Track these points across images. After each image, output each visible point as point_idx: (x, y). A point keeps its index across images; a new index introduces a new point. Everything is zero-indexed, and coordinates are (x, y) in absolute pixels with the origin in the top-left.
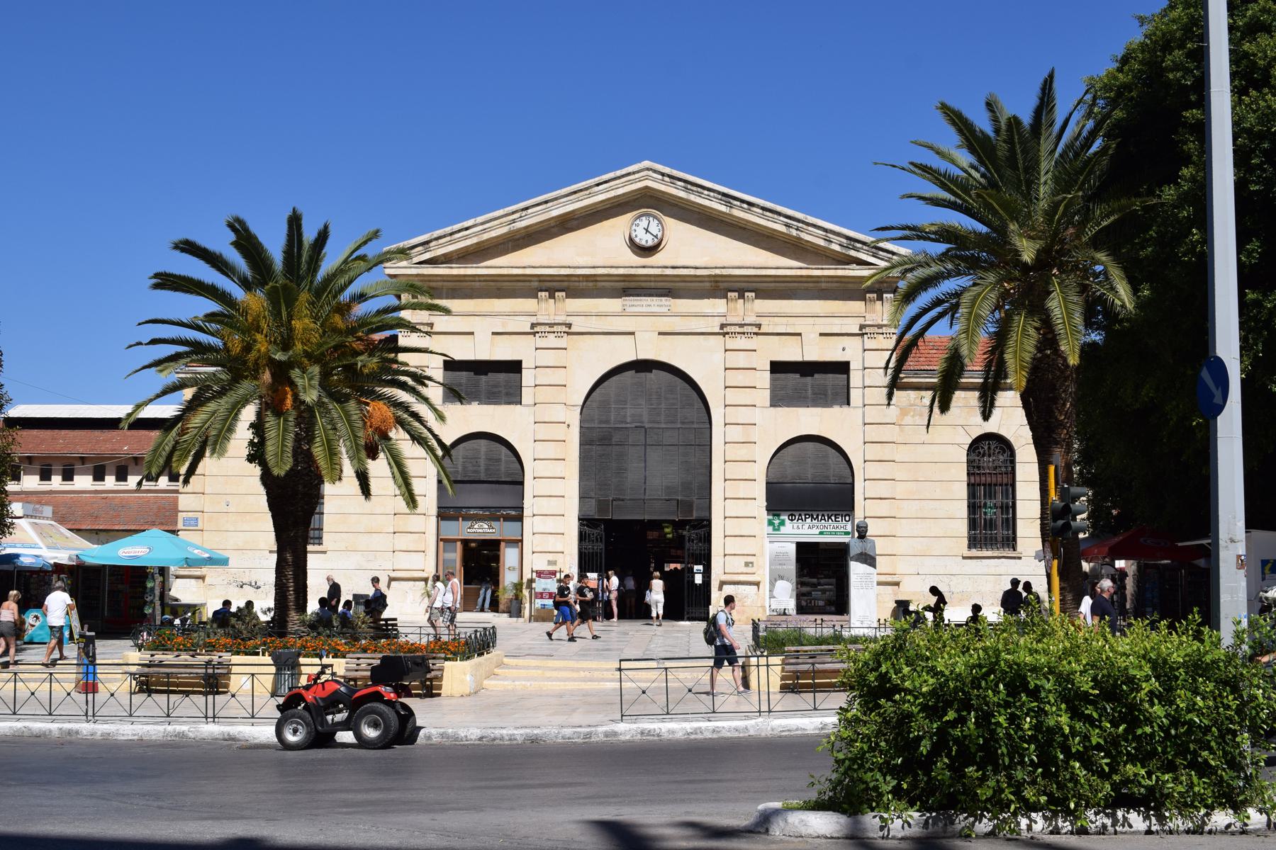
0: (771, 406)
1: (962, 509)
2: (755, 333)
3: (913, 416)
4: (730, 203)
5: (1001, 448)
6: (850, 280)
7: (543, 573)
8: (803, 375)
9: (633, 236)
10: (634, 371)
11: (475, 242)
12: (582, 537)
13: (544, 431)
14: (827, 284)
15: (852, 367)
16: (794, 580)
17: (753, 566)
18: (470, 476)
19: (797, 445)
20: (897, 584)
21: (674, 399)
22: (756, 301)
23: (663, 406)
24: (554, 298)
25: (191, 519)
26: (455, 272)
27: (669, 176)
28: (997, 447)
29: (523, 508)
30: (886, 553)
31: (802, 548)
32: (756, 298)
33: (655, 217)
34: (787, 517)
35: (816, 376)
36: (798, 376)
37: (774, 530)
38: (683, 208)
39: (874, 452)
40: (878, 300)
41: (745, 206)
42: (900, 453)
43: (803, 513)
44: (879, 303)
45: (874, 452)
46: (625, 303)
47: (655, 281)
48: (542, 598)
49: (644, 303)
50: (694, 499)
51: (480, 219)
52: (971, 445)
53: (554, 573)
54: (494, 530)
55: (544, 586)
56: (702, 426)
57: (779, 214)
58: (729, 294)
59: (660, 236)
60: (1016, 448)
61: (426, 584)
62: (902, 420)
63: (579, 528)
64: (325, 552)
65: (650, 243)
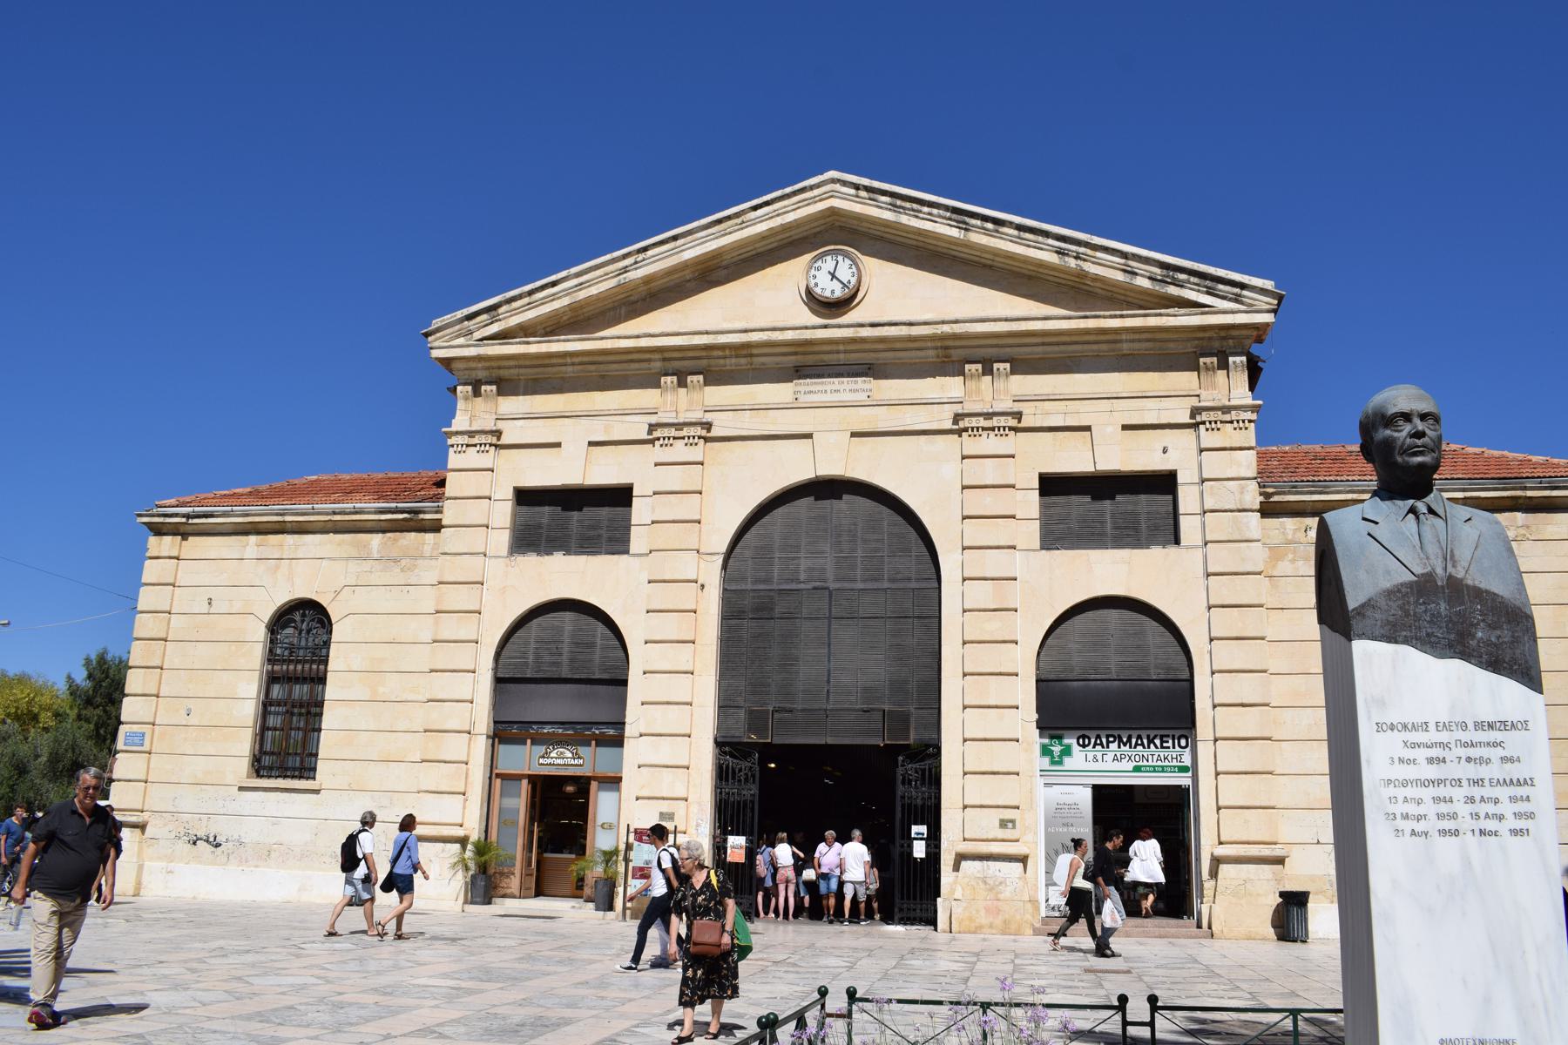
0: (1042, 548)
2: (1011, 429)
3: (1293, 561)
6: (1170, 336)
8: (1097, 497)
10: (812, 498)
12: (723, 774)
14: (1132, 345)
15: (1180, 479)
17: (1014, 827)
19: (1090, 614)
20: (1280, 861)
21: (878, 541)
22: (1011, 377)
23: (859, 553)
25: (135, 734)
26: (533, 349)
27: (868, 189)
30: (1258, 804)
31: (1103, 795)
32: (1013, 372)
33: (846, 255)
34: (1075, 741)
35: (1119, 498)
36: (1087, 499)
38: (891, 242)
39: (1225, 622)
40: (1219, 368)
41: (990, 226)
43: (1103, 734)
44: (1221, 374)
45: (1225, 622)
49: (828, 388)
50: (912, 709)
51: (574, 270)
56: (924, 585)
57: (1046, 234)
61: (464, 848)
62: (1274, 567)
65: (839, 293)
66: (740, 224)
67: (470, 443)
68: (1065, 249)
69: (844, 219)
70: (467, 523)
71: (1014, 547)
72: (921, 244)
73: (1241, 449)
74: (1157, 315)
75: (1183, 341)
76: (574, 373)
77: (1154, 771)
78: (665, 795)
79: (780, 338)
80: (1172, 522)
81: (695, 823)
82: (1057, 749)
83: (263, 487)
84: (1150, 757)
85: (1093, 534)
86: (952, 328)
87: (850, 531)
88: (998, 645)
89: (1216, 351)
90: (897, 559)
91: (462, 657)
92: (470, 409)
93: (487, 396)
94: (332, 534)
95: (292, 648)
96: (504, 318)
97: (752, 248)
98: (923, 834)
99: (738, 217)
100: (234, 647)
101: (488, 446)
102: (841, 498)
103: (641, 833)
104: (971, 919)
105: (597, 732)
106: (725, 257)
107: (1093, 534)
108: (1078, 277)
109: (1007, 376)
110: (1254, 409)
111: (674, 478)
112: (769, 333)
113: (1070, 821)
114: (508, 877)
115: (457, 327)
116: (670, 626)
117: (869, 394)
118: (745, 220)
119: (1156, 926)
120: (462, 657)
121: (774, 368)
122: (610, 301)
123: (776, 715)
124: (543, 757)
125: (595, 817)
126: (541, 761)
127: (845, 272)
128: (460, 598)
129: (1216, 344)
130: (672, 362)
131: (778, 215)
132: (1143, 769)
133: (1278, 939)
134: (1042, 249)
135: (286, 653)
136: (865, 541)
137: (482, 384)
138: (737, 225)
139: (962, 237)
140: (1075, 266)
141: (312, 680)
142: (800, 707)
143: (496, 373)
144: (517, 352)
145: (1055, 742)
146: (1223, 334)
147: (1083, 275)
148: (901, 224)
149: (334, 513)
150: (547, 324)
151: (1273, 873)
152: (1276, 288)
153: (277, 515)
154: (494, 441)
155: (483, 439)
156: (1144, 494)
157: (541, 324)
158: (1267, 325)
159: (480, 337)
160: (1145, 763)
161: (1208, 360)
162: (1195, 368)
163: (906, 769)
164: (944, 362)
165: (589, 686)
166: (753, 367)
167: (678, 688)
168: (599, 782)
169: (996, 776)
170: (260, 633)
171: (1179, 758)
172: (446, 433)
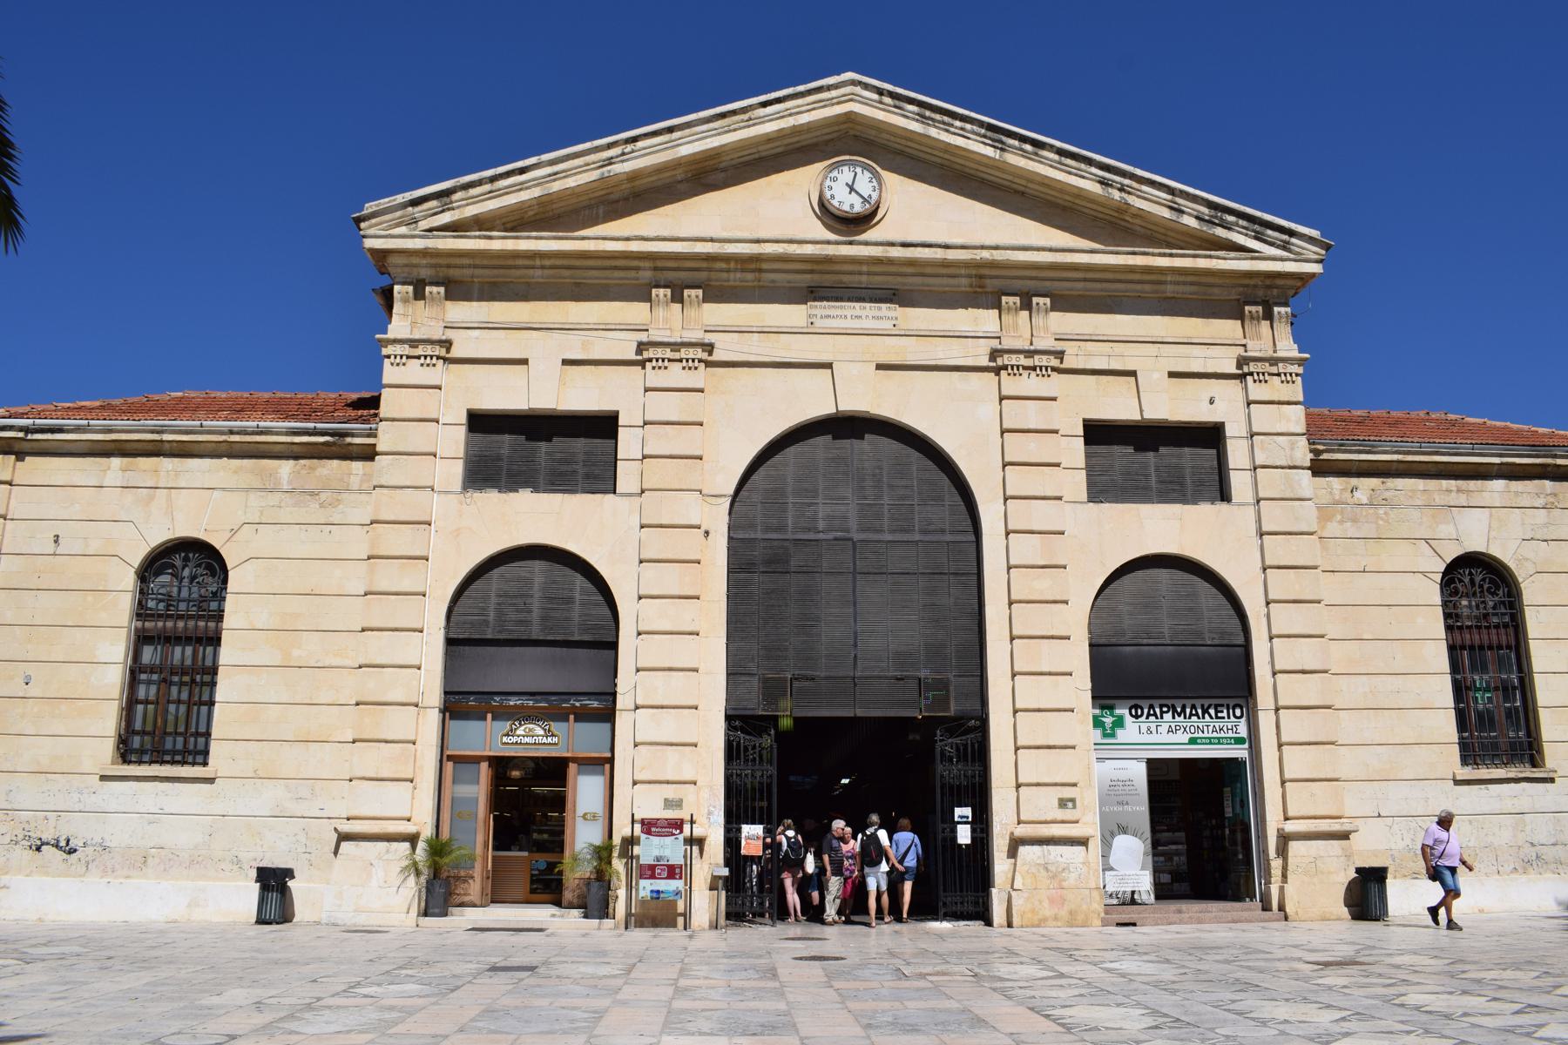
2: (1054, 369)
3: (1341, 522)
4: (1001, 142)
5: (1492, 581)
8: (1141, 448)
9: (828, 194)
10: (830, 436)
12: (732, 752)
13: (657, 544)
14: (1181, 288)
15: (1229, 431)
16: (1148, 834)
17: (1074, 807)
19: (1140, 574)
20: (1345, 836)
21: (906, 487)
23: (886, 500)
24: (681, 301)
27: (892, 95)
28: (1484, 580)
29: (614, 694)
32: (1054, 308)
33: (866, 167)
34: (1128, 711)
35: (1163, 450)
36: (1130, 450)
37: (1105, 735)
38: (911, 157)
39: (1281, 584)
41: (1028, 147)
42: (1327, 587)
43: (1156, 703)
44: (1265, 324)
45: (1281, 584)
46: (814, 312)
47: (869, 274)
48: (653, 877)
49: (849, 313)
50: (951, 676)
52: (1445, 574)
53: (678, 825)
54: (555, 740)
55: (656, 853)
57: (1090, 162)
58: (1004, 299)
59: (875, 196)
60: (1520, 580)
61: (414, 848)
62: (1323, 528)
63: (727, 735)
64: (211, 781)
65: (857, 207)
66: (747, 121)
67: (411, 354)
68: (1109, 180)
69: (859, 128)
70: (410, 450)
71: (1060, 498)
72: (946, 163)
73: (1289, 403)
75: (1228, 287)
76: (542, 278)
77: (1211, 743)
79: (798, 252)
80: (1217, 478)
81: (706, 810)
82: (1108, 720)
83: (117, 402)
85: (1137, 488)
86: (992, 255)
87: (874, 475)
88: (1049, 605)
90: (929, 508)
91: (401, 611)
92: (410, 313)
93: (433, 299)
94: (226, 459)
95: (168, 600)
96: (459, 207)
97: (755, 150)
98: (968, 817)
99: (745, 113)
100: (90, 597)
101: (434, 358)
102: (863, 438)
104: (1033, 911)
105: (578, 704)
106: (724, 158)
107: (1137, 488)
110: (1301, 362)
113: (1125, 799)
114: (465, 881)
115: (399, 214)
117: (894, 322)
119: (1220, 910)
120: (401, 611)
121: (784, 287)
122: (586, 197)
123: (796, 684)
124: (508, 735)
125: (575, 806)
126: (505, 739)
127: (865, 184)
128: (399, 541)
129: (1261, 293)
130: (665, 272)
131: (790, 115)
132: (1199, 741)
133: (1352, 919)
134: (1083, 177)
135: (161, 606)
136: (891, 487)
137: (426, 285)
138: (743, 121)
139: (997, 157)
140: (1119, 199)
141: (199, 640)
142: (823, 674)
143: (443, 272)
144: (477, 247)
145: (1106, 713)
146: (1268, 282)
147: (1124, 208)
148: (929, 137)
149: (231, 432)
150: (508, 219)
151: (1343, 849)
152: (1322, 237)
153: (153, 432)
154: (443, 352)
155: (429, 350)
157: (500, 219)
158: (1313, 275)
159: (427, 227)
160: (1201, 735)
161: (1253, 309)
162: (1239, 316)
163: (945, 744)
164: (975, 292)
165: (565, 649)
166: (761, 283)
168: (579, 765)
170: (129, 580)
171: (1235, 728)
172: (380, 340)
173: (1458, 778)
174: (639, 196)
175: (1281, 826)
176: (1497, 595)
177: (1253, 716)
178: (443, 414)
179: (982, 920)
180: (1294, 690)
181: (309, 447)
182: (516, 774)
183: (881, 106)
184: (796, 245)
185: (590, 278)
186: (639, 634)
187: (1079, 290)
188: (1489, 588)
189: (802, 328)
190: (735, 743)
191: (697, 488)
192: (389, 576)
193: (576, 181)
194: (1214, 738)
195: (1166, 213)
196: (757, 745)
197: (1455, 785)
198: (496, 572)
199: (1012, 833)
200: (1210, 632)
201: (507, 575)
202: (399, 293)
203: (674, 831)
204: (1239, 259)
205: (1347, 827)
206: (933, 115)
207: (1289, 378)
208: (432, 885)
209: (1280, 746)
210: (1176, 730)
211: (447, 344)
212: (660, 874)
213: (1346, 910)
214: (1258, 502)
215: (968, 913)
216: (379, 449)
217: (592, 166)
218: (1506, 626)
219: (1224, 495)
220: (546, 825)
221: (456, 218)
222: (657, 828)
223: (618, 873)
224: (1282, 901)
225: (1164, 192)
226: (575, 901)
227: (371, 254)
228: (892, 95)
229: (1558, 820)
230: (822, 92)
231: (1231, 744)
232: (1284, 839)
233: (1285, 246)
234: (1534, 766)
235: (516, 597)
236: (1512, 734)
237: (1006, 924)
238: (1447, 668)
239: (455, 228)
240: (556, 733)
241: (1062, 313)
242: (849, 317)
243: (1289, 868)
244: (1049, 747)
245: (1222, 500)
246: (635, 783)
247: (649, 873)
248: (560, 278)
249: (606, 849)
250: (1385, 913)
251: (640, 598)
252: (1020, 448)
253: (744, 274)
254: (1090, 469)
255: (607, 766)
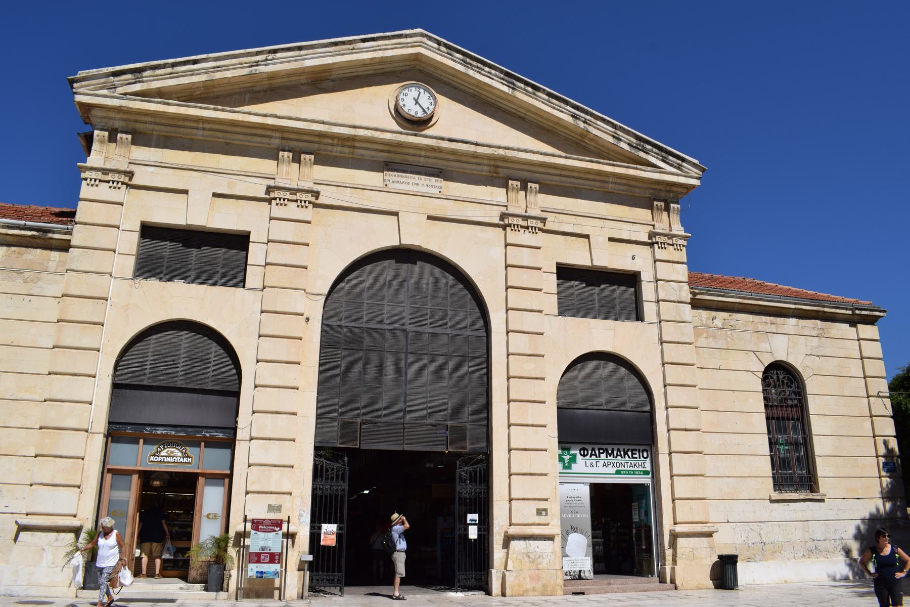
1: (762, 444)
2: (540, 229)
3: (707, 338)
5: (788, 379)
7: (262, 524)
9: (401, 103)
10: (394, 261)
11: (203, 80)
12: (318, 473)
13: (272, 324)
14: (617, 187)
15: (644, 277)
16: (590, 533)
17: (546, 515)
18: (161, 381)
19: (588, 363)
20: (709, 535)
21: (443, 298)
23: (429, 306)
26: (172, 109)
27: (446, 46)
28: (784, 378)
29: (235, 429)
30: (697, 496)
31: (598, 491)
32: (540, 192)
33: (426, 90)
34: (579, 451)
35: (603, 286)
36: (583, 284)
38: (455, 88)
41: (530, 89)
43: (596, 447)
44: (665, 214)
45: (674, 374)
47: (425, 157)
48: (258, 561)
49: (411, 181)
50: (467, 425)
52: (764, 373)
53: (278, 524)
54: (190, 460)
55: (262, 544)
58: (510, 182)
59: (431, 108)
60: (805, 379)
61: (77, 537)
62: (696, 340)
63: (315, 461)
65: (420, 114)
66: (351, 49)
67: (103, 179)
68: (577, 115)
69: (423, 65)
70: (96, 246)
71: (541, 312)
72: (476, 93)
73: (678, 263)
74: (634, 168)
76: (203, 136)
77: (629, 474)
78: (273, 490)
80: (634, 306)
81: (298, 514)
82: (567, 458)
84: (626, 464)
85: (587, 309)
87: (422, 289)
88: (533, 380)
89: (662, 199)
91: (81, 362)
93: (122, 143)
96: (147, 81)
97: (354, 70)
98: (476, 521)
99: (350, 44)
101: (120, 184)
102: (416, 264)
103: (257, 522)
104: (520, 585)
105: (208, 435)
106: (334, 73)
107: (587, 309)
108: (581, 136)
109: (536, 193)
110: (686, 238)
111: (282, 231)
112: (373, 132)
115: (103, 80)
116: (279, 349)
118: (355, 47)
120: (81, 362)
122: (238, 87)
124: (154, 455)
125: (201, 508)
126: (152, 458)
127: (425, 100)
130: (289, 141)
131: (380, 50)
132: (622, 472)
133: (715, 588)
134: (562, 112)
136: (433, 297)
137: (118, 132)
138: (349, 49)
139: (510, 93)
142: (382, 421)
143: (132, 125)
145: (565, 453)
146: (668, 188)
154: (126, 180)
155: (116, 177)
156: (618, 285)
158: (694, 186)
159: (123, 92)
160: (623, 468)
161: (659, 203)
162: (651, 207)
163: (463, 471)
164: (492, 176)
166: (354, 156)
167: (285, 400)
169: (534, 477)
171: (643, 464)
172: (80, 167)
173: (773, 498)
174: (274, 90)
175: (672, 528)
176: (791, 387)
177: (655, 457)
178: (123, 223)
179: (484, 591)
180: (680, 441)
181: (19, 238)
182: (157, 483)
183: (439, 52)
184: (379, 132)
185: (237, 140)
186: (256, 387)
187: (556, 182)
188: (787, 383)
189: (380, 187)
190: (319, 466)
191: (302, 288)
192: (72, 335)
193: (232, 74)
194: (631, 471)
195: (611, 140)
196: (335, 468)
197: (770, 503)
198: (153, 338)
199: (506, 532)
200: (630, 402)
201: (162, 340)
202: (98, 136)
203: (275, 529)
204: (653, 172)
205: (712, 529)
206: (472, 62)
207: (679, 248)
208: (90, 566)
209: (672, 476)
210: (608, 465)
211: (130, 175)
212: (263, 560)
213: (711, 582)
214: (660, 322)
215: (469, 586)
216: (72, 243)
217: (244, 65)
218: (796, 406)
219: (639, 316)
220: (177, 521)
221: (144, 88)
222: (263, 526)
223: (232, 558)
224: (672, 577)
225: (610, 126)
226: (198, 578)
227: (79, 107)
228: (446, 46)
229: (827, 525)
230: (401, 38)
231: (641, 475)
232: (674, 536)
233: (679, 167)
234: (812, 492)
235: (167, 356)
236: (799, 472)
237: (501, 594)
238: (766, 432)
239: (144, 95)
240: (190, 455)
241: (545, 195)
242: (411, 184)
243: (677, 556)
244: (531, 474)
245: (637, 319)
246: (247, 493)
247: (256, 559)
248: (216, 138)
249: (224, 541)
250: (737, 585)
251: (258, 361)
252: (517, 277)
253: (343, 148)
254: (559, 294)
255: (227, 480)
